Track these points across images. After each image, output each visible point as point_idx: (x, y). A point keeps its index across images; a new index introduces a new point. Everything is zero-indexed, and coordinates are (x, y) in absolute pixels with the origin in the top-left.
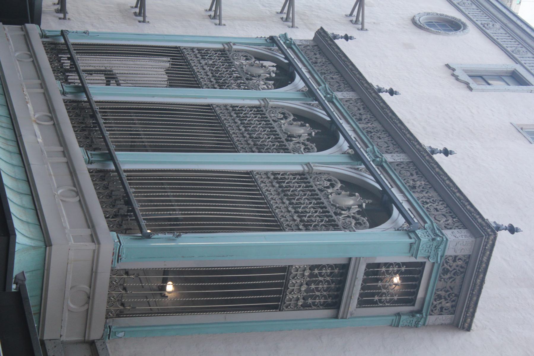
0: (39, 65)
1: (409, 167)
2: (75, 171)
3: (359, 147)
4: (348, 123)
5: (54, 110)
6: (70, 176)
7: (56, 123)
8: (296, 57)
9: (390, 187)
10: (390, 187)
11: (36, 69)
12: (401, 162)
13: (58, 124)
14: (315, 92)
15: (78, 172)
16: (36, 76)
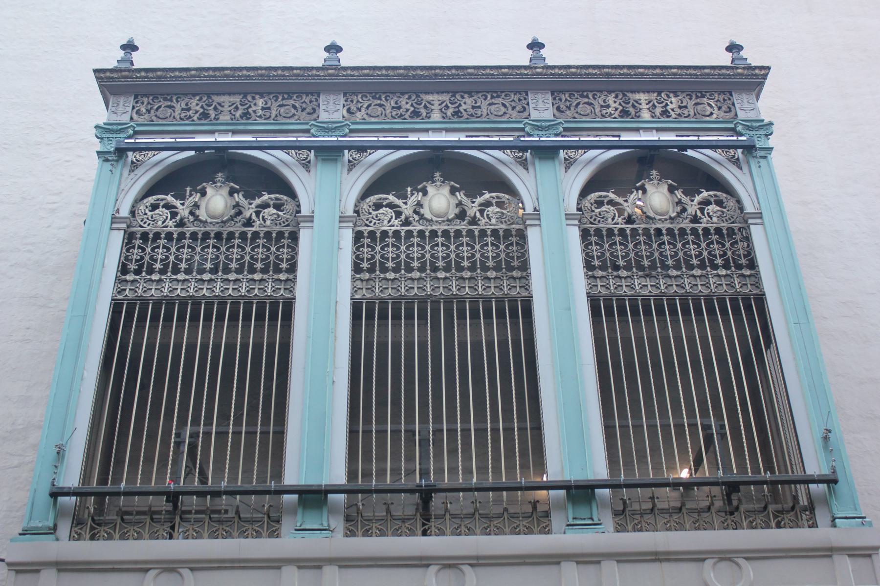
0: (232, 561)
1: (566, 100)
2: (656, 553)
3: (497, 139)
4: (426, 130)
5: (421, 558)
6: (665, 565)
7: (475, 562)
8: (256, 135)
9: (617, 139)
10: (617, 139)
11: (226, 568)
12: (553, 105)
13: (477, 558)
14: (542, 144)
15: (661, 548)
16: (271, 572)
